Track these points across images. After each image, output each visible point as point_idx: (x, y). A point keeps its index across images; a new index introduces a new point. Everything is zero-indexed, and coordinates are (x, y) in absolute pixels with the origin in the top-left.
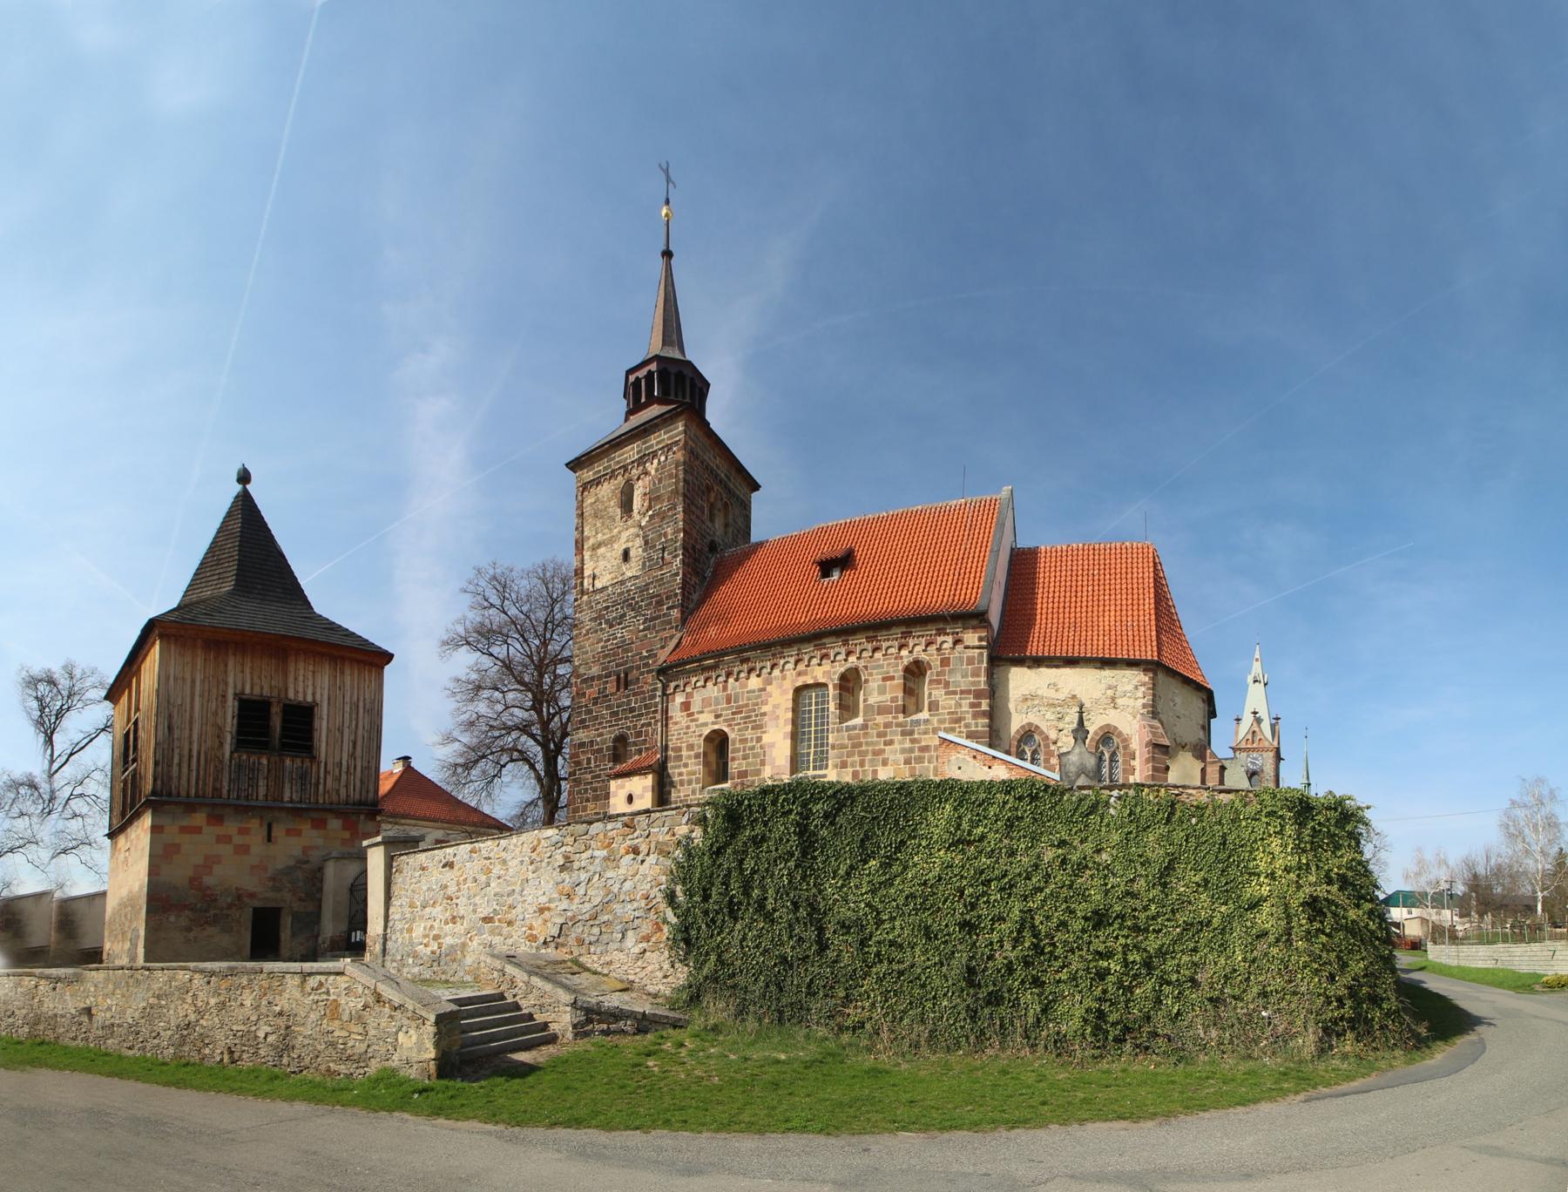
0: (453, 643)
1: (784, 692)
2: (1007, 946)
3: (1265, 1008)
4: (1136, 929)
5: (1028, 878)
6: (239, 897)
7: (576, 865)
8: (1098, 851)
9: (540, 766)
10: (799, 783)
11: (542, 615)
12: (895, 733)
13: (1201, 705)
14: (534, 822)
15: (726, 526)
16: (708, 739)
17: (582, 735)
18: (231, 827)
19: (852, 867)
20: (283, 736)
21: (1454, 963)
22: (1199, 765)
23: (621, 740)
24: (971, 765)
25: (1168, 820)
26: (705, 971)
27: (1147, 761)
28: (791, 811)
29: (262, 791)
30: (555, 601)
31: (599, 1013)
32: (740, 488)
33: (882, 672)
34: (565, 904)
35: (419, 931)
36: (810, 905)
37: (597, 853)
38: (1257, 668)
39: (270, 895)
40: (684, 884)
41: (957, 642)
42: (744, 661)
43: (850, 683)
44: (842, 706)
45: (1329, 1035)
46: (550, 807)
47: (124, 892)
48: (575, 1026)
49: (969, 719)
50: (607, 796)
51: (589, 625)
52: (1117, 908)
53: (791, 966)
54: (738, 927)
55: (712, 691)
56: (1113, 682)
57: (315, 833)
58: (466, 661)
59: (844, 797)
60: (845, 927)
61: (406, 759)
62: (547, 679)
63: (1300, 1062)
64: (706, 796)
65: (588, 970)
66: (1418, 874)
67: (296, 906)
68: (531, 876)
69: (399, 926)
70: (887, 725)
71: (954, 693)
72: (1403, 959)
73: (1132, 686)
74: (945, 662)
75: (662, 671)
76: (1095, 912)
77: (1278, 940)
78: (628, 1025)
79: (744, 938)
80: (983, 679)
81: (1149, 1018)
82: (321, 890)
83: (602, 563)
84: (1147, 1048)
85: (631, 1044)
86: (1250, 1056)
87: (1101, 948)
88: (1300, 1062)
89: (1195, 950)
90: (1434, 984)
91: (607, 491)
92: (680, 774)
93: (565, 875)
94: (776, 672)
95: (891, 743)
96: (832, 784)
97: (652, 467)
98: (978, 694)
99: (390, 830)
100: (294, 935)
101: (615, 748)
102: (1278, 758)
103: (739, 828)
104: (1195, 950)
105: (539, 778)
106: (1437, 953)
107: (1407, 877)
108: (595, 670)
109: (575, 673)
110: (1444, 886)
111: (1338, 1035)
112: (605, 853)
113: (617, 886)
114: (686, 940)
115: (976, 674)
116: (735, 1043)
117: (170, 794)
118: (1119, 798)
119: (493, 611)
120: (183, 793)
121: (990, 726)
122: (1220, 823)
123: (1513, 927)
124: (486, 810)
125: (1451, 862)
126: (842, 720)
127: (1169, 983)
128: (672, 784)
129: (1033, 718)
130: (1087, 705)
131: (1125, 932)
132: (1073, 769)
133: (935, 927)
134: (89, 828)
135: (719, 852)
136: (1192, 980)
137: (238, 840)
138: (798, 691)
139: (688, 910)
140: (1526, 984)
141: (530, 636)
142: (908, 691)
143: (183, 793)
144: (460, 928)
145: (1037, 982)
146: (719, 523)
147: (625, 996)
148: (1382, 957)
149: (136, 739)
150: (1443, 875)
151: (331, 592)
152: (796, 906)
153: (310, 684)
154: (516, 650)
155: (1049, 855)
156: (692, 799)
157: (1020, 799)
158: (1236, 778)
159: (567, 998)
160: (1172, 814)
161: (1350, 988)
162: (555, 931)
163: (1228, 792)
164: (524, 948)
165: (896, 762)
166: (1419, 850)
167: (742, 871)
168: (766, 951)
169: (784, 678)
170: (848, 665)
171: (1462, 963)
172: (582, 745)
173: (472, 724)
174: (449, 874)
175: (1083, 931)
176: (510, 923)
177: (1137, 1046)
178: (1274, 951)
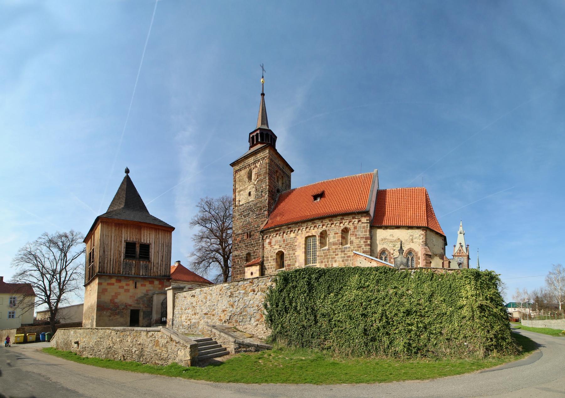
0: (194, 223)
1: (302, 238)
2: (377, 322)
3: (466, 342)
4: (421, 316)
5: (384, 299)
6: (126, 306)
7: (234, 295)
8: (408, 290)
9: (222, 263)
10: (307, 268)
11: (222, 214)
12: (339, 251)
13: (442, 241)
14: (221, 281)
15: (283, 184)
16: (277, 254)
17: (236, 253)
18: (123, 283)
19: (325, 296)
20: (140, 254)
21: (530, 326)
22: (441, 261)
23: (249, 254)
24: (364, 262)
25: (431, 280)
26: (277, 330)
27: (424, 260)
28: (305, 277)
29: (133, 272)
30: (227, 209)
31: (243, 345)
32: (286, 170)
33: (334, 230)
34: (231, 309)
35: (184, 318)
36: (312, 308)
37: (241, 291)
38: (461, 229)
39: (136, 305)
40: (270, 301)
41: (359, 221)
42: (289, 228)
43: (323, 235)
44: (321, 243)
45: (488, 351)
46: (226, 276)
47: (89, 304)
48: (235, 349)
50: (244, 273)
51: (238, 217)
52: (414, 309)
53: (306, 329)
54: (288, 315)
55: (278, 238)
56: (412, 234)
57: (150, 285)
58: (198, 229)
59: (322, 273)
60: (323, 315)
61: (179, 262)
62: (224, 235)
63: (478, 360)
64: (277, 273)
65: (239, 330)
66: (517, 297)
67: (144, 309)
68: (220, 299)
69: (177, 316)
70: (336, 249)
71: (358, 238)
72: (513, 325)
73: (418, 234)
74: (355, 228)
75: (262, 232)
76: (407, 310)
77: (469, 319)
78: (252, 349)
79: (290, 319)
80: (368, 233)
81: (426, 346)
82: (152, 304)
83: (242, 197)
84: (425, 356)
85: (254, 355)
86: (461, 358)
87: (409, 322)
88: (478, 360)
89: (441, 323)
90: (524, 333)
91: (243, 173)
93: (231, 299)
94: (300, 232)
95: (337, 255)
96: (318, 268)
97: (258, 165)
98: (366, 238)
99: (174, 285)
100: (143, 319)
101: (247, 257)
102: (469, 259)
103: (288, 283)
104: (441, 323)
105: (222, 267)
106: (524, 323)
107: (513, 298)
108: (240, 232)
109: (233, 232)
110: (526, 301)
111: (491, 351)
112: (244, 291)
113: (248, 302)
114: (271, 320)
115: (366, 232)
116: (288, 354)
117: (104, 273)
118: (414, 272)
119: (206, 213)
120: (108, 272)
121: (371, 249)
122: (449, 280)
123: (551, 314)
124: (205, 277)
125: (529, 293)
127: (432, 334)
128: (265, 269)
129: (385, 246)
130: (403, 242)
131: (417, 317)
132: (399, 263)
133: (353, 316)
134: (78, 283)
135: (281, 291)
136: (441, 333)
137: (126, 287)
139: (271, 310)
140: (556, 333)
141: (219, 221)
142: (343, 238)
143: (108, 272)
144: (197, 317)
145: (388, 334)
146: (280, 183)
147: (252, 339)
148: (505, 325)
149: (93, 255)
150: (526, 297)
151: (155, 208)
152: (307, 308)
153: (148, 237)
154: (214, 225)
155: (391, 291)
156: (272, 274)
157: (381, 273)
158: (454, 265)
159: (232, 340)
160: (432, 277)
161: (495, 335)
162: (228, 318)
163: (452, 270)
164: (218, 323)
165: (339, 261)
166: (518, 289)
167: (289, 297)
168: (297, 323)
169: (302, 234)
170: (323, 229)
171: (534, 326)
172: (236, 256)
173: (200, 249)
174: (193, 300)
175: (403, 317)
176: (213, 315)
177: (422, 355)
178: (468, 323)
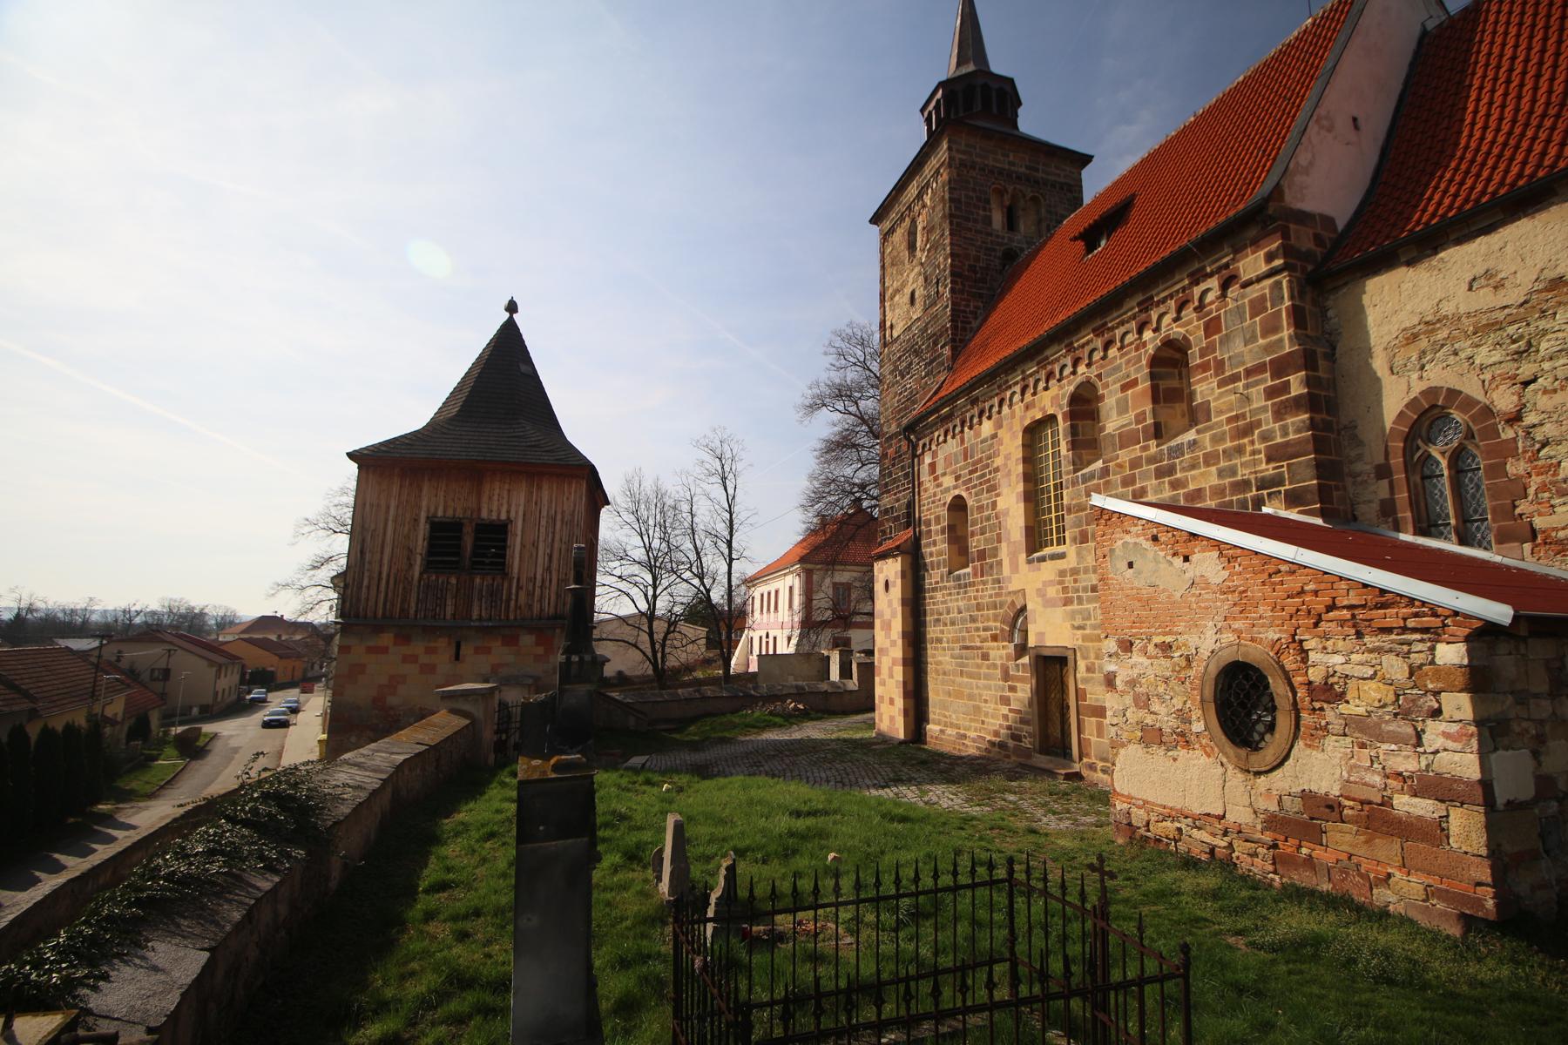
12: (1145, 476)
41: (1225, 286)
42: (974, 402)
43: (1084, 405)
44: (1074, 445)
49: (1269, 423)
55: (952, 446)
70: (1135, 464)
71: (1235, 378)
74: (1212, 327)
80: (1286, 333)
92: (931, 555)
94: (1005, 409)
98: (1280, 367)
126: (1078, 464)
138: (1034, 433)
169: (1013, 416)
170: (1079, 379)
